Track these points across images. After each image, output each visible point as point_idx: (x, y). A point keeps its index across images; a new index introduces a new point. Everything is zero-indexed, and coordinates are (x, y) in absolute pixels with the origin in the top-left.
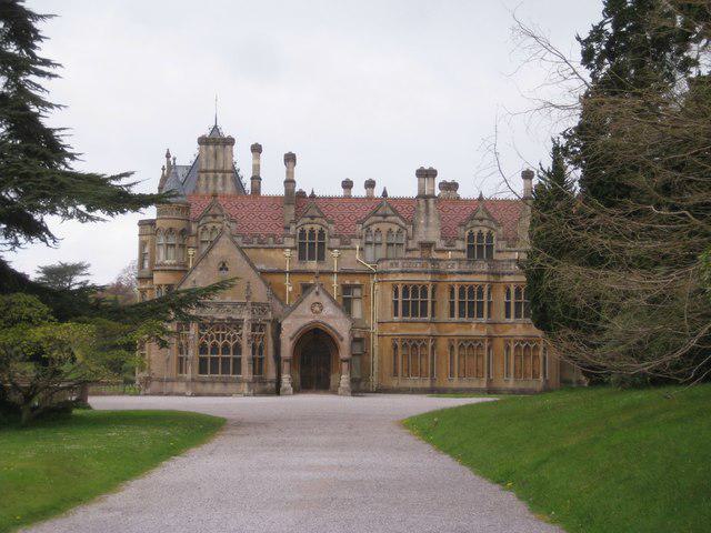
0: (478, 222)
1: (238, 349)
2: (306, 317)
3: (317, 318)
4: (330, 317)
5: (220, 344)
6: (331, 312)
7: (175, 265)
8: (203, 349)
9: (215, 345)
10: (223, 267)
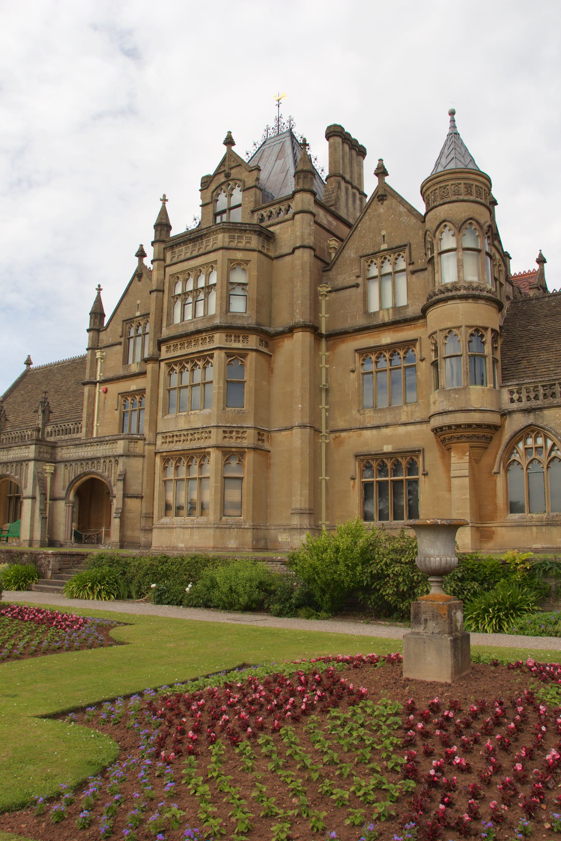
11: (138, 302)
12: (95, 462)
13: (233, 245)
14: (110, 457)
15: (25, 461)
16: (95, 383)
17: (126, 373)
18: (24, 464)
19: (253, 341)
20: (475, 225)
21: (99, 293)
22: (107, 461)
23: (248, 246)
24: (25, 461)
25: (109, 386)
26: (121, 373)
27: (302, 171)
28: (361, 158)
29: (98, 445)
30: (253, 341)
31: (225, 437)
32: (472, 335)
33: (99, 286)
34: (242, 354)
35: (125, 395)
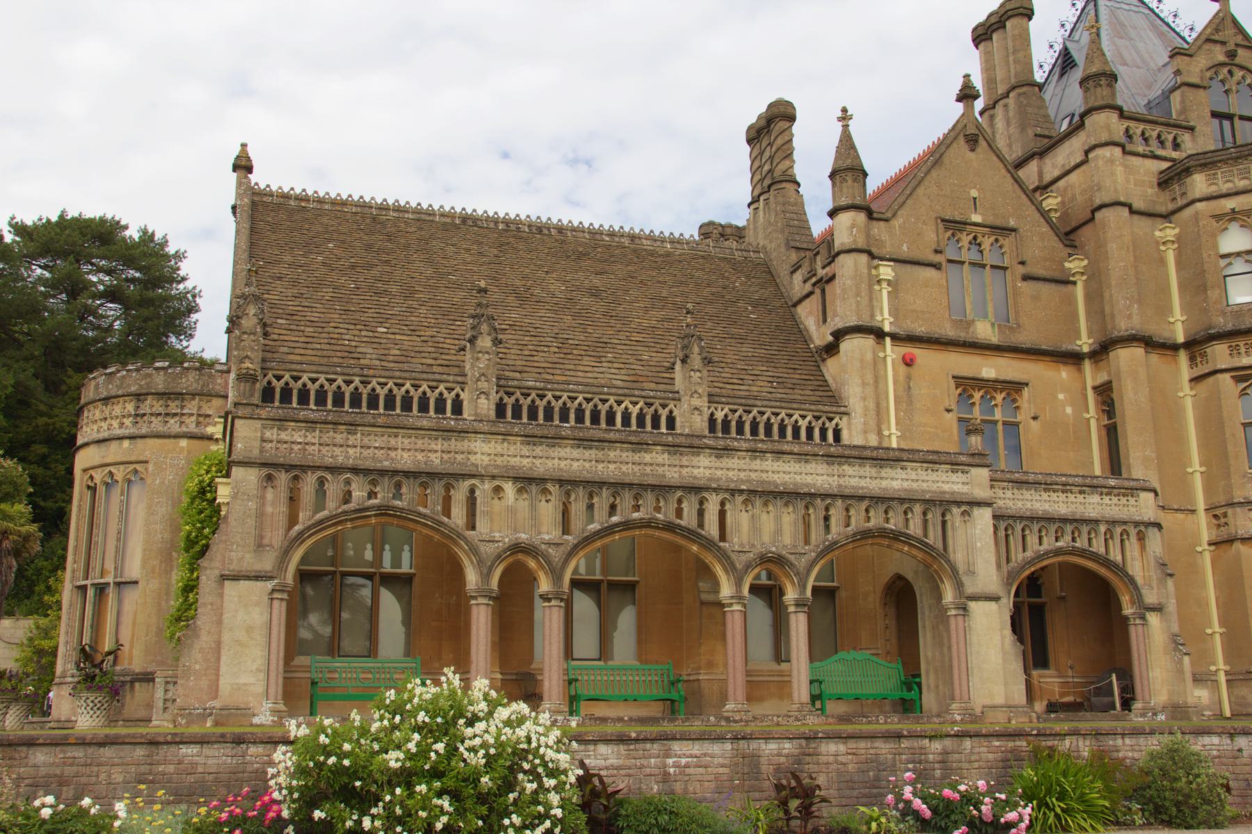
11: (974, 193)
12: (1085, 529)
14: (1125, 523)
15: (958, 504)
16: (879, 334)
17: (962, 335)
18: (956, 511)
21: (846, 127)
22: (1119, 530)
24: (958, 504)
25: (922, 355)
26: (950, 332)
29: (1084, 492)
33: (844, 110)
35: (966, 384)
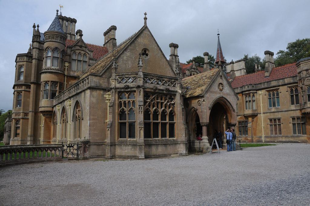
0: (193, 70)
1: (172, 115)
2: (215, 92)
3: (221, 95)
4: (228, 94)
5: (160, 110)
6: (228, 91)
7: (58, 70)
8: (147, 115)
9: (156, 112)
10: (145, 52)
13: (20, 61)
19: (24, 88)
20: (50, 49)
23: (24, 60)
27: (36, 35)
28: (73, 23)
30: (24, 88)
31: (16, 116)
32: (45, 84)
34: (21, 92)
